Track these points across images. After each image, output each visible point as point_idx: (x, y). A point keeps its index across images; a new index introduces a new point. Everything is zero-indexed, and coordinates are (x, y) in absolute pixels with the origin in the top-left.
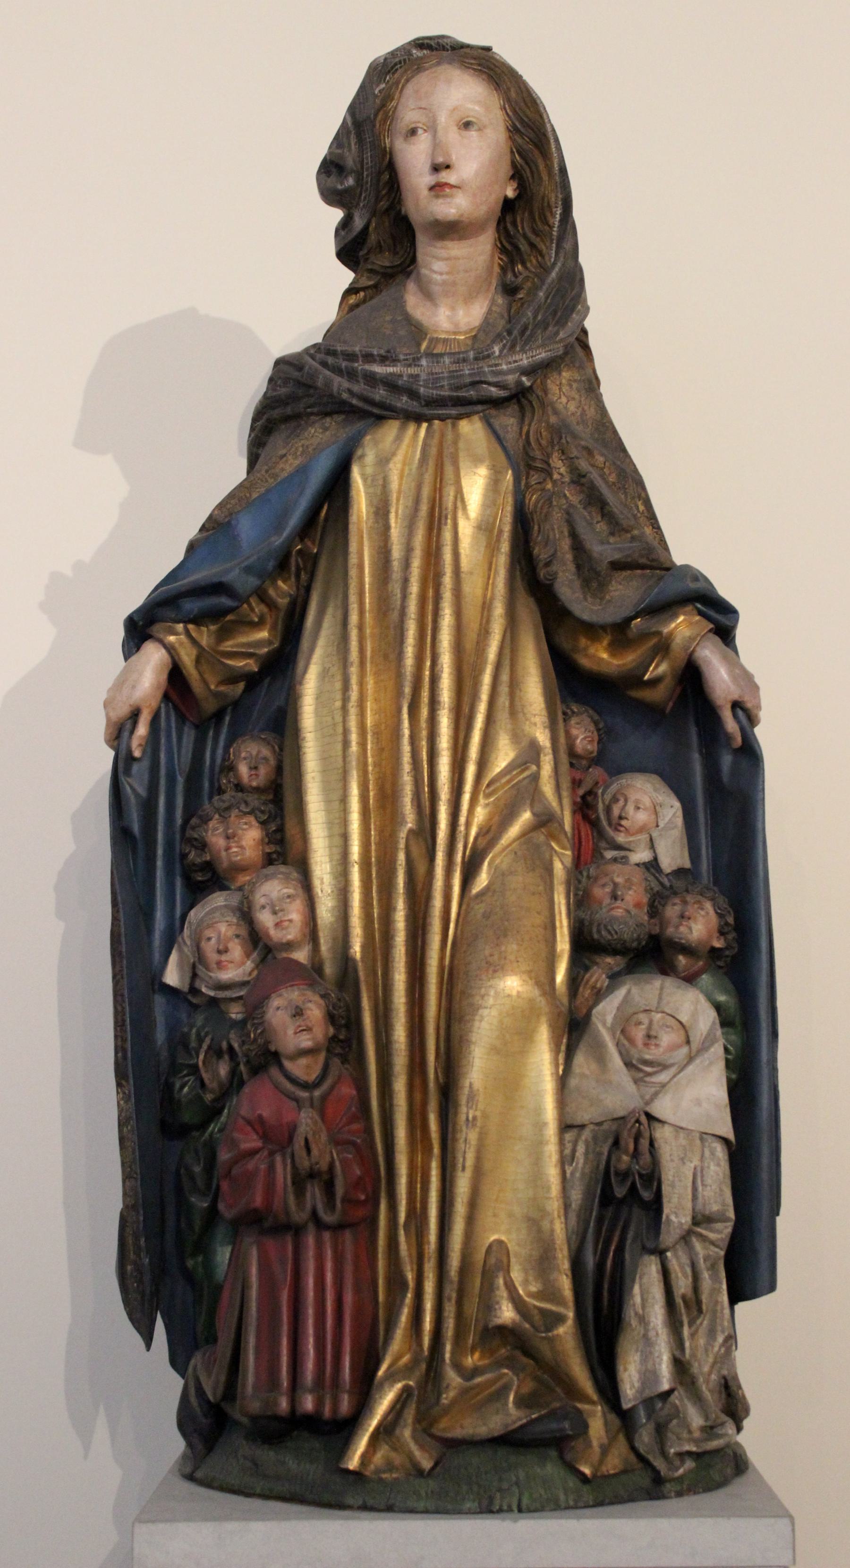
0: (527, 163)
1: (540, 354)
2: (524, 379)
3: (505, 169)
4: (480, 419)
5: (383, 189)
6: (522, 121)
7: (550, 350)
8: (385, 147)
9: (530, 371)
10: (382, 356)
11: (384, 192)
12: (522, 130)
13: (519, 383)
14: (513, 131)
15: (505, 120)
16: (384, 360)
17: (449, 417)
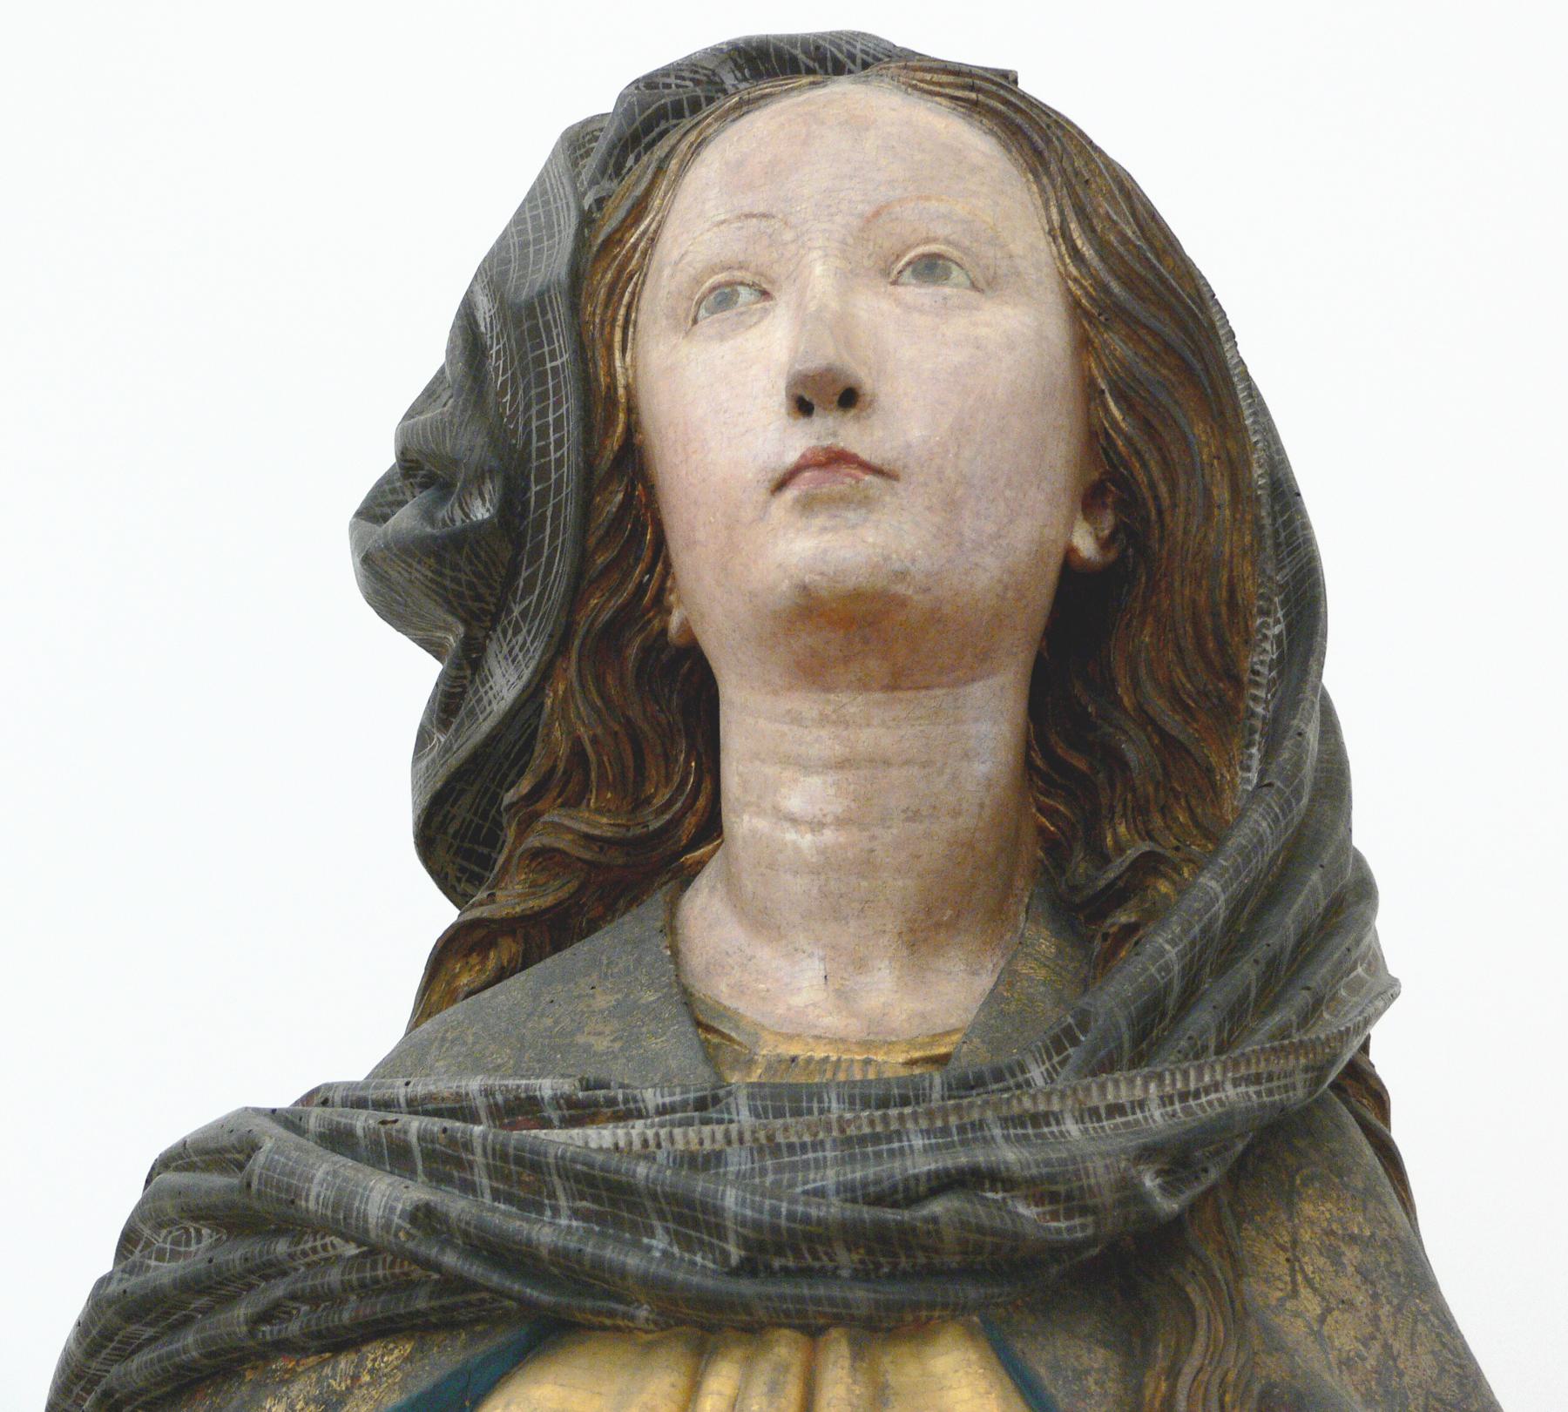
0: (1147, 426)
1: (1216, 1087)
2: (1150, 1182)
3: (1059, 453)
4: (971, 1334)
5: (602, 543)
6: (1129, 281)
7: (1257, 1079)
8: (612, 387)
9: (1176, 1158)
10: (571, 1103)
11: (600, 560)
12: (1134, 306)
13: (1129, 1192)
14: (1090, 316)
15: (1064, 277)
16: (579, 1112)
17: (842, 1317)
